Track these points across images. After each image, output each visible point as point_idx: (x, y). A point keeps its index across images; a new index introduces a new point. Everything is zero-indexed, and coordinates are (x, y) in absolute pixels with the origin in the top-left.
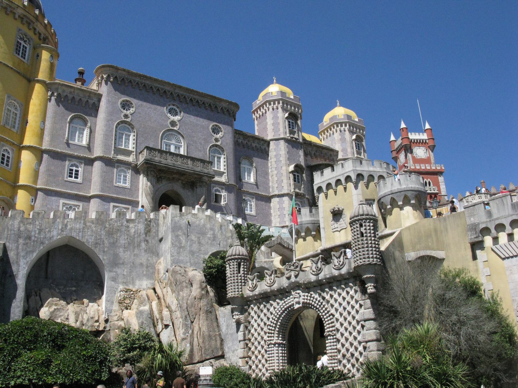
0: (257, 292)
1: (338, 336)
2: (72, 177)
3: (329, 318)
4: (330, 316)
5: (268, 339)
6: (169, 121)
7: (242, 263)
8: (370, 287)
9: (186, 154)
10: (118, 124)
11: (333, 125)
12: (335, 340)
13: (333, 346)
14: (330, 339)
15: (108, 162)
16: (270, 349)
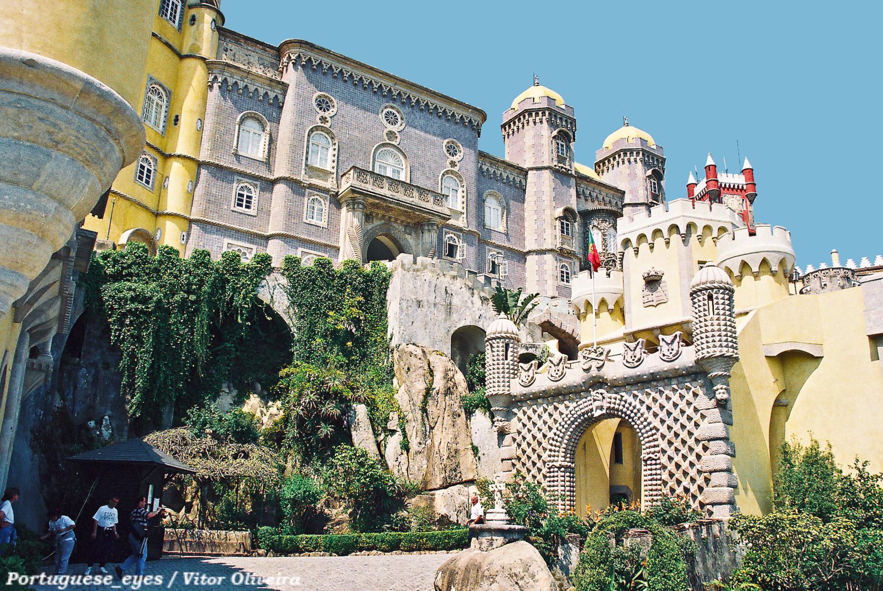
0: (535, 388)
1: (664, 460)
2: (241, 205)
3: (650, 433)
4: (651, 429)
5: (549, 459)
6: (386, 131)
7: (511, 345)
8: (720, 391)
9: (408, 182)
10: (312, 131)
11: (618, 153)
12: (658, 466)
13: (656, 474)
14: (651, 465)
15: (295, 185)
16: (552, 474)
